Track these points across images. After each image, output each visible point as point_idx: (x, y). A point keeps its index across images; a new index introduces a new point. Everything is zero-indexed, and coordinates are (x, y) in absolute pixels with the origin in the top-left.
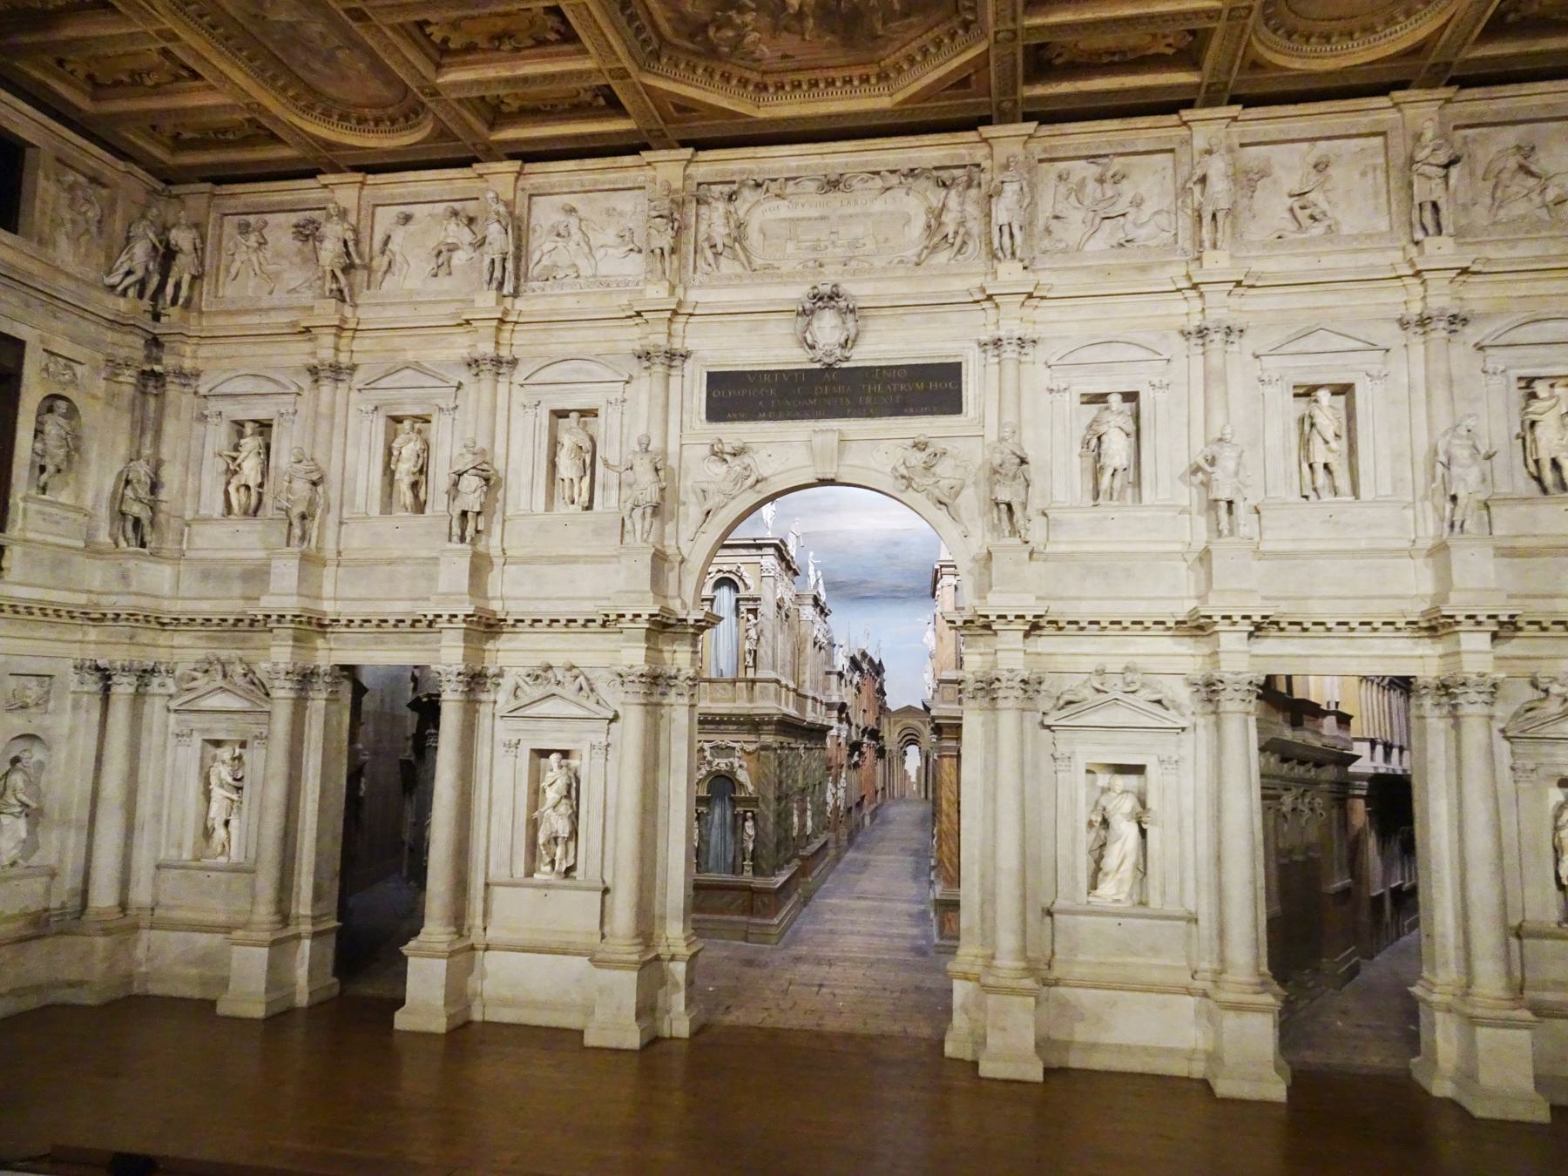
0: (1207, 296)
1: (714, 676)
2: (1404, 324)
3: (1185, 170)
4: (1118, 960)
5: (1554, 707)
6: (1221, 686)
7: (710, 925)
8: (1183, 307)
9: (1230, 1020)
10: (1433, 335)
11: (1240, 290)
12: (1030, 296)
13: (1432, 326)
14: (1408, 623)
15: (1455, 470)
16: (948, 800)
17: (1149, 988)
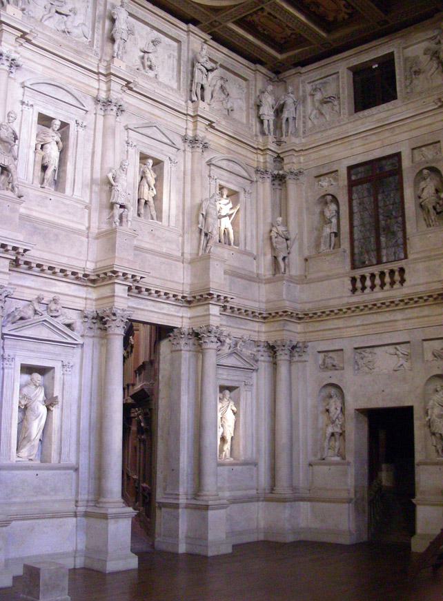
0: (112, 83)
2: (185, 139)
3: (100, 9)
4: (35, 499)
5: (226, 349)
6: (107, 318)
8: (96, 84)
9: (112, 526)
10: (197, 150)
11: (125, 89)
12: (22, 37)
13: (198, 145)
14: (183, 297)
15: (210, 220)
17: (55, 515)
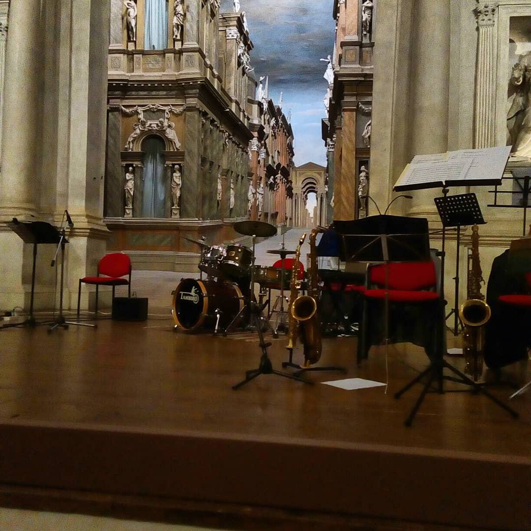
1: (147, 48)
7: (142, 259)
16: (347, 149)
